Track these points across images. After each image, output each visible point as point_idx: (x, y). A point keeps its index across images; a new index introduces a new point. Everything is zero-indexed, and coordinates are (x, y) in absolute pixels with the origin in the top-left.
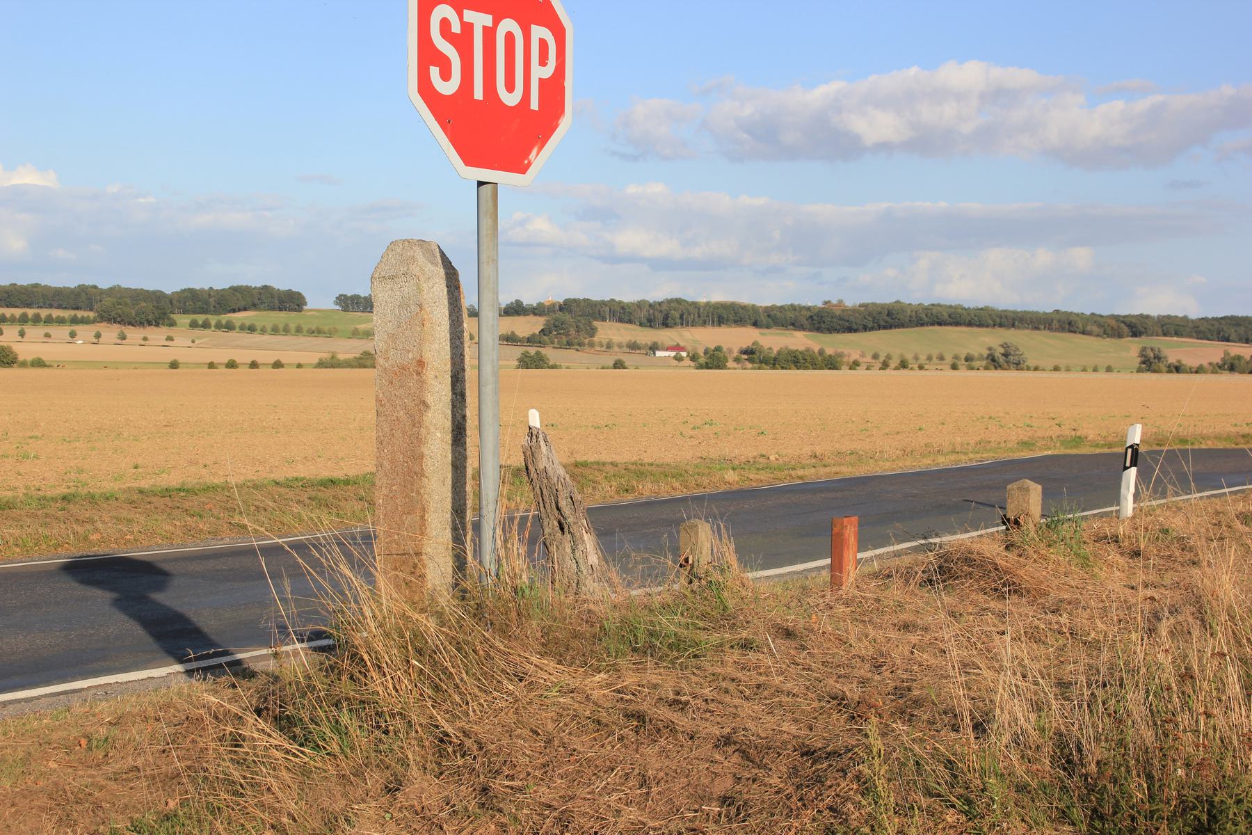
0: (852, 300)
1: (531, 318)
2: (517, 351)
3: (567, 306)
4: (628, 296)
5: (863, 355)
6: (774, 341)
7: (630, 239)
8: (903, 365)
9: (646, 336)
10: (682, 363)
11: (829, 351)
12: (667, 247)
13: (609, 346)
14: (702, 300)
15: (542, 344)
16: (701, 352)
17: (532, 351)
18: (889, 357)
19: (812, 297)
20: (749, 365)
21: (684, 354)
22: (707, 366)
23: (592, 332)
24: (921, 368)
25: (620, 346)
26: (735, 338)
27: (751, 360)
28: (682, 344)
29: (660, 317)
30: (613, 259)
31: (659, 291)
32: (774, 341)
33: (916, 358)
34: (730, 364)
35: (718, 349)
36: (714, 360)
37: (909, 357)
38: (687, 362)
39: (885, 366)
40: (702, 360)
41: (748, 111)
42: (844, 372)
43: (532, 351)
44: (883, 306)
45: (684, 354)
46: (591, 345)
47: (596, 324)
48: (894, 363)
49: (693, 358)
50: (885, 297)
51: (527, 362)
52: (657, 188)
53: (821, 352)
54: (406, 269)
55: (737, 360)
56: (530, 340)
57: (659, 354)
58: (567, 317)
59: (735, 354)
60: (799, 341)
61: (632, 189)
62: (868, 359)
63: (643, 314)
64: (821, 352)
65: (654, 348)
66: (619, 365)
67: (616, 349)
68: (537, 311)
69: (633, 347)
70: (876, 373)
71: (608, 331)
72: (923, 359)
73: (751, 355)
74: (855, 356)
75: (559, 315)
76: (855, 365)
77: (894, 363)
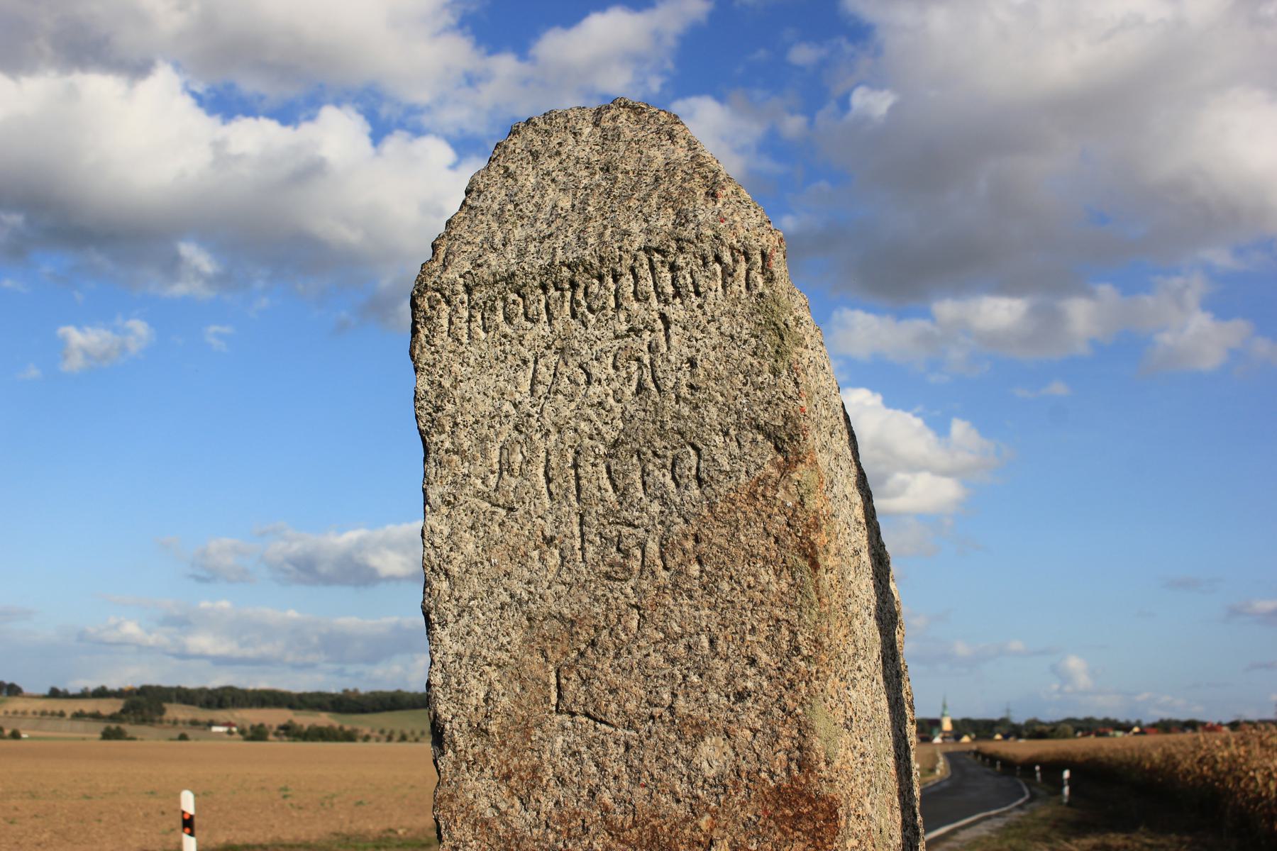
0: (364, 688)
1: (113, 700)
2: (101, 726)
3: (145, 691)
4: (191, 683)
5: (372, 731)
6: (305, 719)
7: (202, 642)
8: (403, 738)
9: (203, 715)
10: (234, 737)
11: (347, 728)
12: (227, 648)
13: (175, 722)
14: (251, 687)
15: (122, 721)
16: (248, 727)
17: (113, 726)
18: (392, 733)
19: (334, 686)
20: (285, 738)
21: (234, 729)
22: (252, 739)
23: (162, 711)
24: (417, 740)
25: (184, 722)
26: (274, 717)
27: (287, 735)
28: (233, 721)
29: (216, 701)
30: (184, 656)
31: (216, 681)
32: (305, 719)
33: (413, 733)
34: (271, 737)
35: (262, 725)
36: (258, 734)
37: (407, 732)
38: (237, 736)
39: (390, 739)
40: (249, 734)
41: (296, 547)
42: (359, 745)
43: (113, 726)
44: (387, 694)
45: (234, 729)
46: (161, 722)
47: (166, 705)
48: (397, 736)
49: (242, 732)
50: (388, 687)
51: (107, 735)
52: (225, 604)
53: (341, 728)
54: (665, 221)
55: (276, 734)
56: (113, 718)
57: (215, 729)
58: (142, 699)
59: (275, 729)
60: (324, 719)
61: (205, 604)
62: (376, 734)
63: (203, 698)
64: (341, 728)
65: (211, 724)
66: (183, 737)
67: (180, 725)
68: (119, 694)
69: (194, 723)
70: (383, 745)
71: (176, 712)
72: (418, 733)
73: (288, 731)
74: (366, 731)
75: (137, 698)
76: (367, 738)
77: (397, 736)
